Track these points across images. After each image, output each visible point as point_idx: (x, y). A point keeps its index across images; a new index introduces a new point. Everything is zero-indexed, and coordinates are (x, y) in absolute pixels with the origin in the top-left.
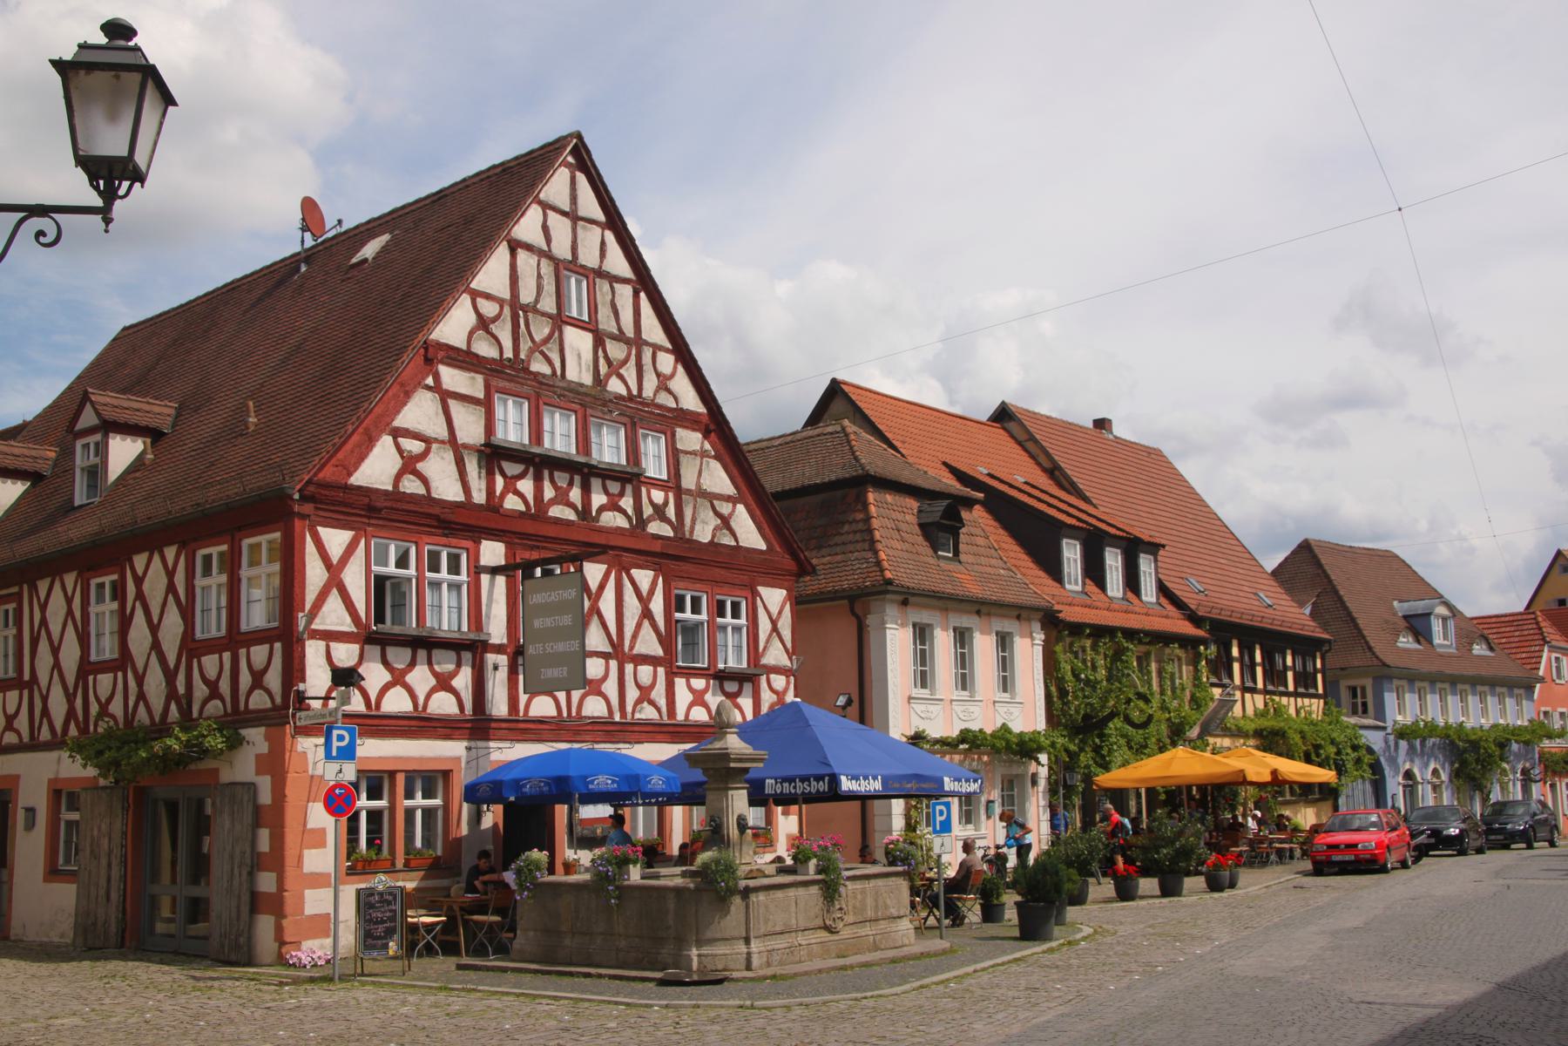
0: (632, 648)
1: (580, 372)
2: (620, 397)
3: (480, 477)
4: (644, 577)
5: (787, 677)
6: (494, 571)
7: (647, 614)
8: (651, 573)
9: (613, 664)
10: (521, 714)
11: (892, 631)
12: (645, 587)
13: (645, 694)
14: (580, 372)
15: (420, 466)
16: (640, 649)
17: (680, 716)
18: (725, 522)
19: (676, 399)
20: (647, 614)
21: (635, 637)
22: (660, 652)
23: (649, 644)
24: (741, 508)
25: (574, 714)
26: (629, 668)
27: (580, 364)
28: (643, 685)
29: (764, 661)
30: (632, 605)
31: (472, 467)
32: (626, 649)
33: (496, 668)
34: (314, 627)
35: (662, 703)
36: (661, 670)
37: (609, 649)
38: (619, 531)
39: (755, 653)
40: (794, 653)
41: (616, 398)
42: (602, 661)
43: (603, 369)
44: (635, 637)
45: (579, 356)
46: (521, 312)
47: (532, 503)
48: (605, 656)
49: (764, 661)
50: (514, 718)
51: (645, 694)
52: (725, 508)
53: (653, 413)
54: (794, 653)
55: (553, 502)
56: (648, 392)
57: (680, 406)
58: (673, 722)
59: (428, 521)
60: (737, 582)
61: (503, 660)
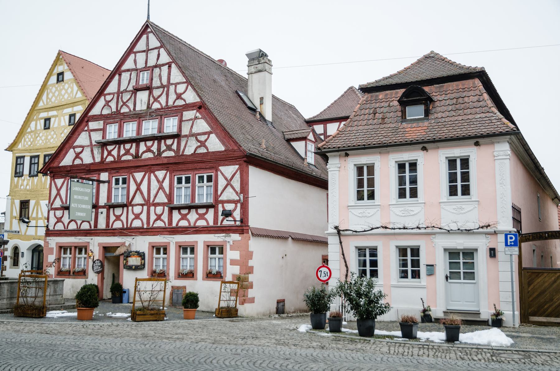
0: (154, 201)
1: (141, 106)
2: (158, 109)
3: (98, 154)
4: (161, 174)
5: (236, 204)
6: (104, 182)
7: (161, 188)
8: (165, 172)
9: (145, 208)
10: (110, 227)
11: (332, 172)
12: (161, 177)
13: (159, 217)
14: (141, 106)
15: (80, 155)
16: (157, 201)
17: (174, 225)
18: (203, 144)
19: (185, 101)
20: (161, 188)
21: (155, 197)
22: (166, 201)
23: (162, 198)
24: (213, 136)
25: (129, 226)
26: (152, 208)
27: (141, 103)
28: (158, 214)
29: (220, 199)
30: (155, 185)
31: (96, 151)
32: (151, 201)
33: (102, 213)
34: (52, 207)
35: (166, 220)
36: (166, 209)
37: (143, 202)
38: (150, 159)
39: (216, 196)
40: (241, 193)
41: (155, 110)
42: (141, 207)
43: (152, 100)
44: (155, 197)
45: (141, 101)
46: (120, 94)
47: (116, 158)
48: (142, 205)
49: (220, 199)
50: (107, 229)
51: (159, 217)
52: (202, 138)
53: (173, 110)
54: (241, 193)
55: (124, 155)
56: (170, 103)
57: (187, 102)
58: (171, 227)
59: (82, 171)
60: (208, 167)
61: (104, 211)
